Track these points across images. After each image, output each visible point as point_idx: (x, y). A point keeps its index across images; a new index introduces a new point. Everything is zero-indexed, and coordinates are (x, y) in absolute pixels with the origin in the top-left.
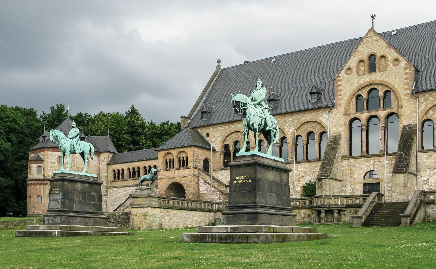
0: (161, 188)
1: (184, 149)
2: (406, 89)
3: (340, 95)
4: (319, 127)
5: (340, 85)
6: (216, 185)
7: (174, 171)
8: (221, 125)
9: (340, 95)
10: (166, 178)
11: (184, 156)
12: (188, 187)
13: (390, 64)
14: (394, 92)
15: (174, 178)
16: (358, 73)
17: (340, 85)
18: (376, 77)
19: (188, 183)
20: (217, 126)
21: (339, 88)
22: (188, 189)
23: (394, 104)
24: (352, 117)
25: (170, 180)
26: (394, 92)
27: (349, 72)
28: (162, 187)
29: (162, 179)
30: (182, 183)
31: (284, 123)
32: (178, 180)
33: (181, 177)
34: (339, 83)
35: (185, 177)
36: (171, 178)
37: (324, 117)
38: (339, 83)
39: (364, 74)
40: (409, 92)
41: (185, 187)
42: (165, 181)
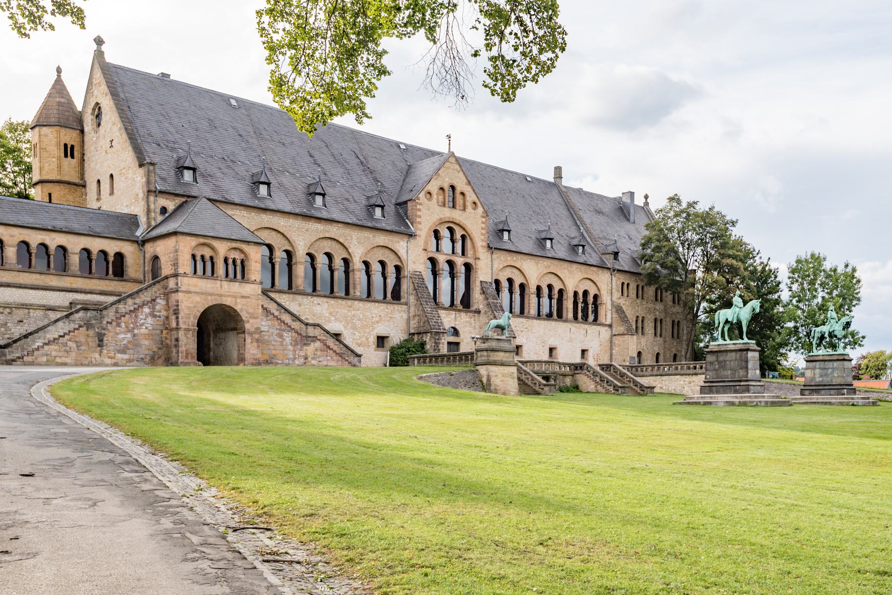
0: (187, 311)
1: (244, 247)
2: (482, 240)
3: (420, 223)
4: (393, 256)
5: (420, 210)
6: (287, 318)
7: (219, 282)
8: (241, 208)
9: (420, 223)
10: (202, 293)
11: (237, 257)
12: (250, 317)
13: (469, 204)
14: (471, 239)
15: (221, 295)
16: (438, 202)
17: (420, 210)
18: (456, 215)
19: (251, 311)
20: (232, 206)
21: (418, 213)
22: (251, 321)
23: (470, 252)
24: (431, 255)
25: (209, 298)
26: (471, 239)
27: (428, 196)
28: (189, 308)
29: (189, 292)
30: (238, 308)
31: (348, 238)
32: (228, 301)
33: (235, 297)
34: (418, 207)
35: (243, 297)
36: (211, 295)
37: (401, 245)
38: (418, 207)
39: (444, 206)
40: (485, 244)
41: (244, 316)
42: (197, 298)
